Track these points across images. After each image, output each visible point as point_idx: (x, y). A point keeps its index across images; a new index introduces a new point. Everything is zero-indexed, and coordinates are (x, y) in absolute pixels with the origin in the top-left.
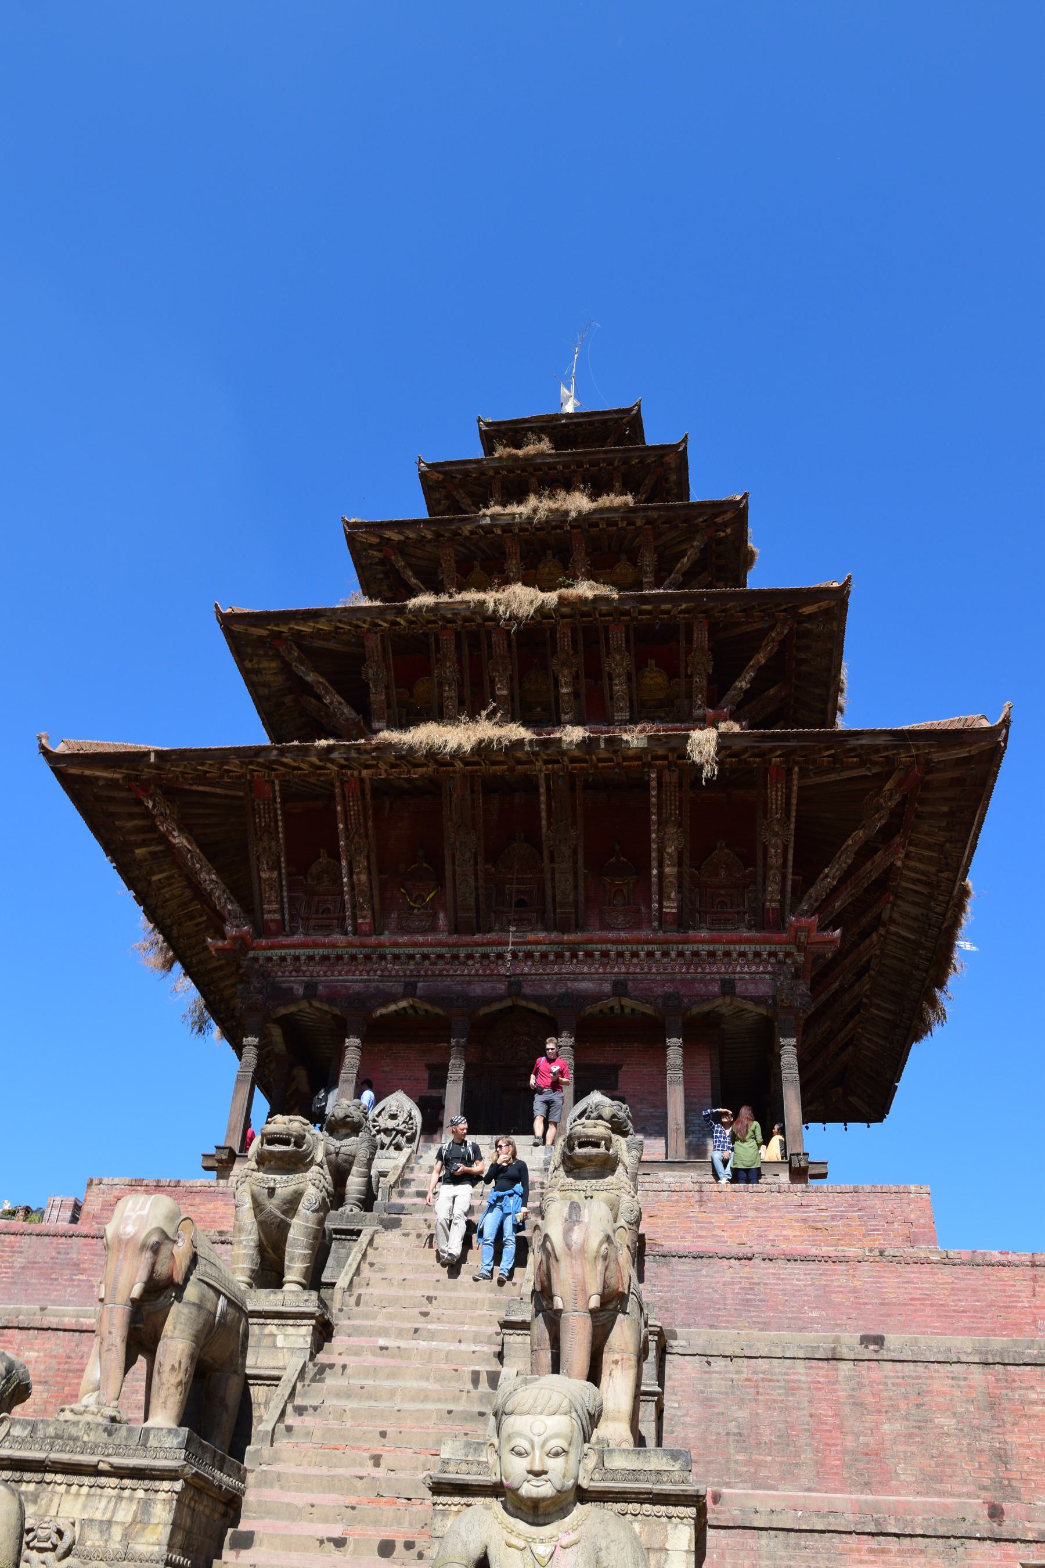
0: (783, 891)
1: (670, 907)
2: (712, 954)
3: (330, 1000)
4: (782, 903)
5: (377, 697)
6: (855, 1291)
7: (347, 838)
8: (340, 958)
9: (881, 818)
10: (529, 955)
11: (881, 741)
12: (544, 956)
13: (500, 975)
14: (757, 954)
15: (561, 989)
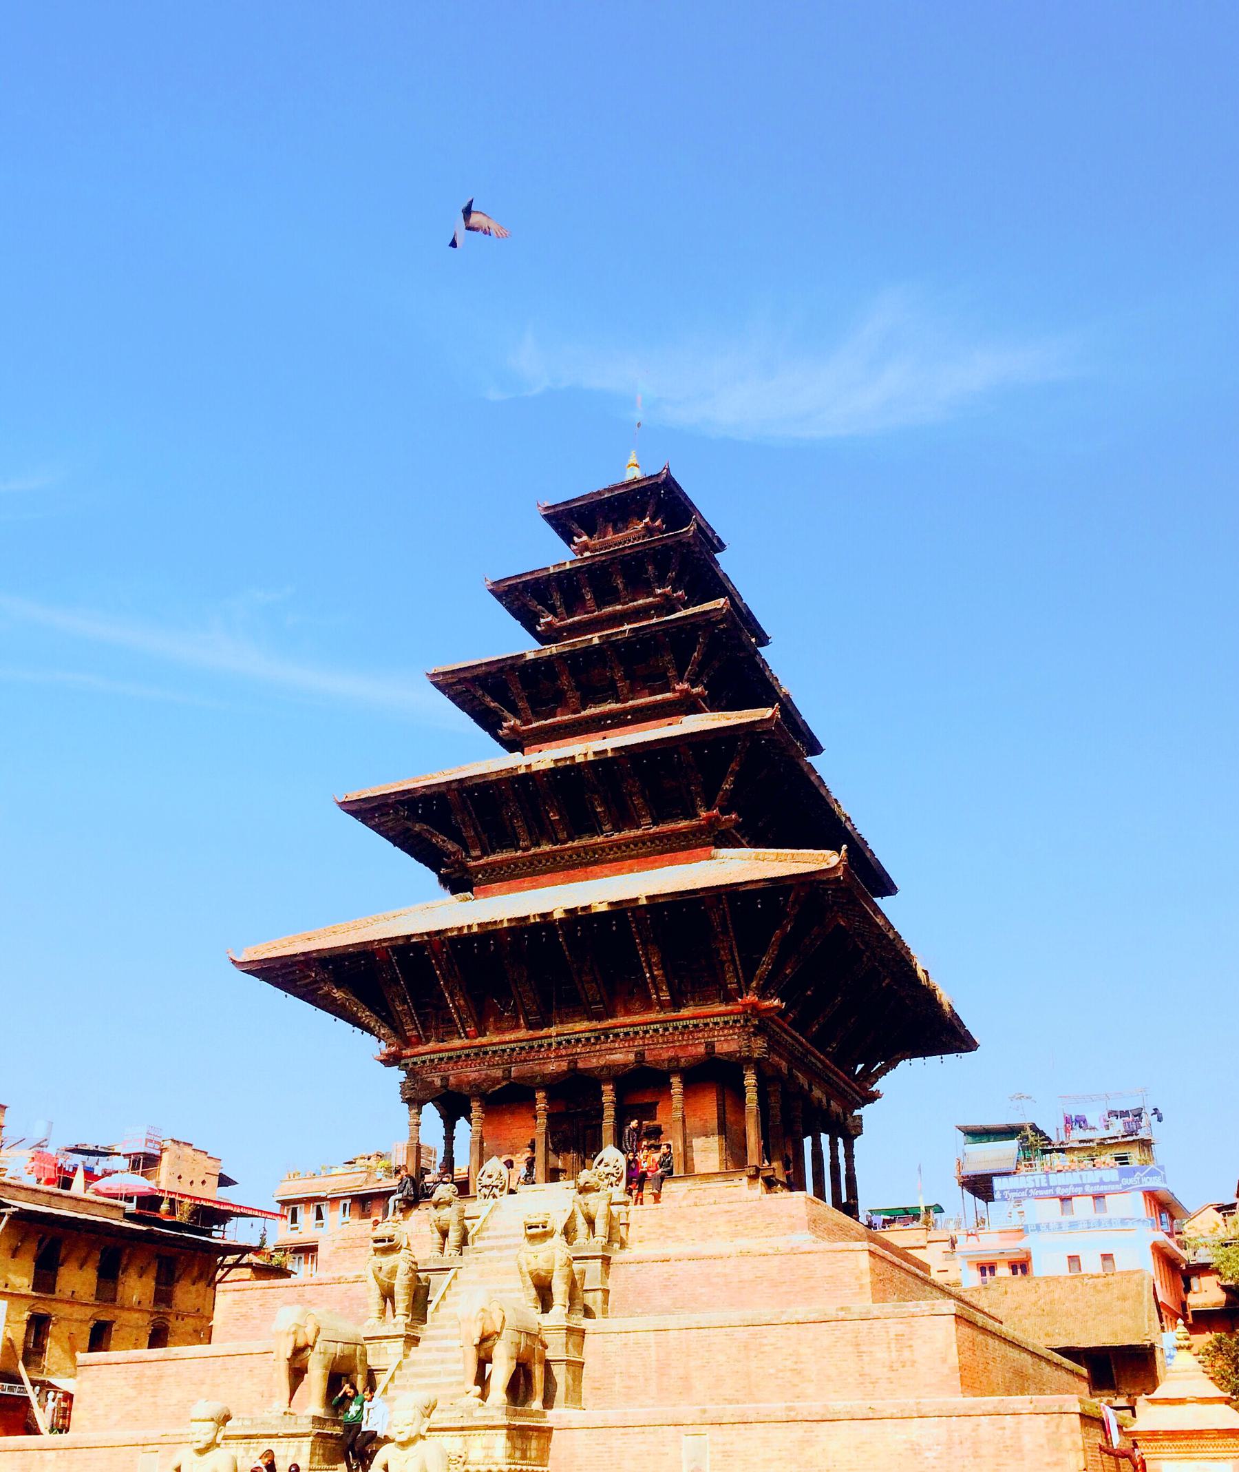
0: (737, 976)
1: (665, 996)
2: (696, 1026)
3: (458, 1086)
4: (738, 982)
5: (469, 833)
6: (725, 1275)
7: (444, 979)
8: (459, 1057)
9: (788, 923)
10: (578, 1040)
11: (761, 885)
12: (588, 1039)
13: (562, 1056)
14: (726, 1023)
15: (602, 1062)
